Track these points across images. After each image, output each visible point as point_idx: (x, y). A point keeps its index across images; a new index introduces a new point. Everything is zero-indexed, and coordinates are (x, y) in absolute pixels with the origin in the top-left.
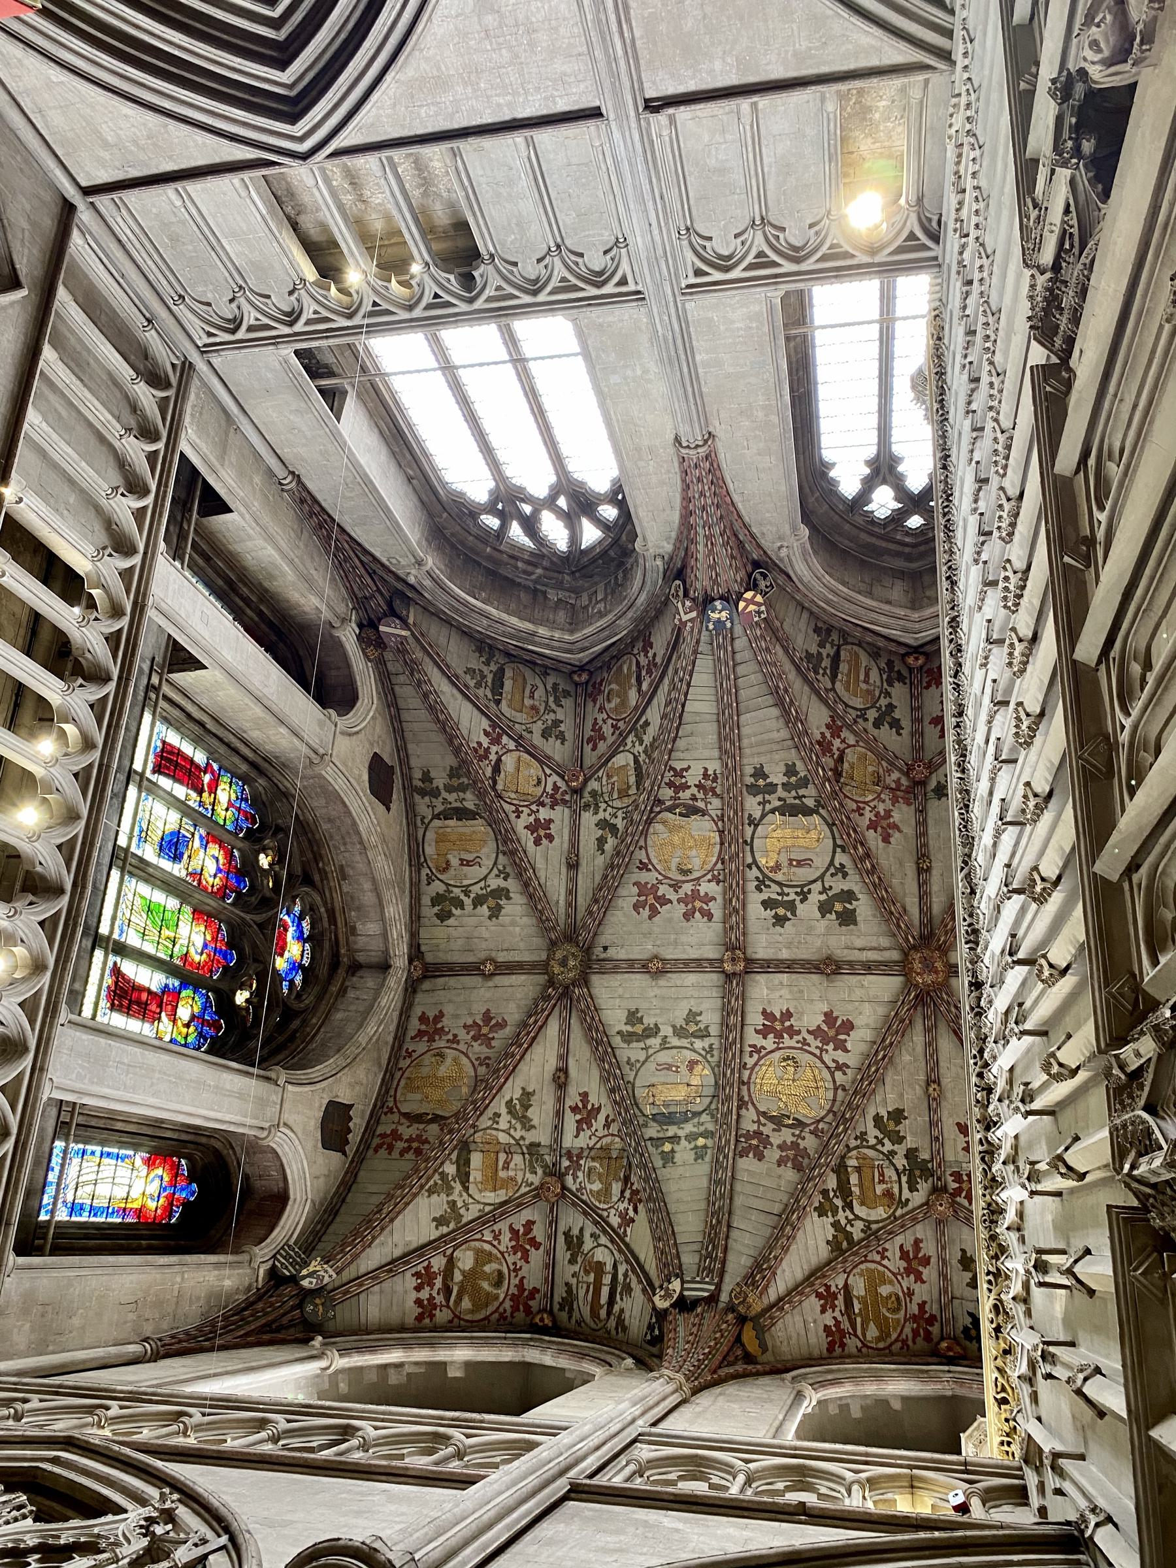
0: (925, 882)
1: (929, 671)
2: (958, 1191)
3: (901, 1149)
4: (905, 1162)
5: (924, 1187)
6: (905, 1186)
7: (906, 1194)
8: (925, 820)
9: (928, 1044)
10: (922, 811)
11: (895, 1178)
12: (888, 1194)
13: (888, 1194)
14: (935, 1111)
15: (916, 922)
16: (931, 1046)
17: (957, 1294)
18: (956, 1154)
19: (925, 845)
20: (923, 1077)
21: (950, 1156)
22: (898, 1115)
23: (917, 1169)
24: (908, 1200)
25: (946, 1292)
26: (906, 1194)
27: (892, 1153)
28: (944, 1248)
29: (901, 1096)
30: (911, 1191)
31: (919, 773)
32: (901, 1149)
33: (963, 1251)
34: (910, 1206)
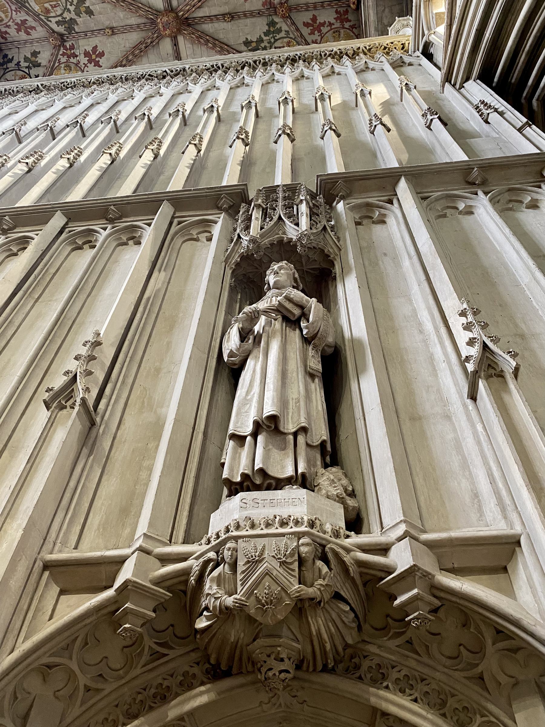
0: (218, 19)
1: (347, 12)
2: (65, 48)
3: (73, 15)
4: (68, 18)
5: (61, 29)
6: (57, 19)
7: (54, 20)
8: (254, 16)
9: (131, 26)
10: (259, 14)
11: (58, 13)
12: (48, 11)
13: (48, 11)
14: (99, 33)
15: (195, 15)
16: (128, 29)
17: (21, 50)
18: (83, 46)
19: (239, 18)
20: (115, 25)
21: (81, 42)
22: (89, 12)
23: (70, 24)
24: (51, 21)
25: (20, 44)
26: (54, 20)
27: (69, 11)
28: (37, 42)
29: (100, 13)
30: (56, 22)
31: (280, 11)
32: (73, 15)
33: (39, 53)
34: (49, 23)
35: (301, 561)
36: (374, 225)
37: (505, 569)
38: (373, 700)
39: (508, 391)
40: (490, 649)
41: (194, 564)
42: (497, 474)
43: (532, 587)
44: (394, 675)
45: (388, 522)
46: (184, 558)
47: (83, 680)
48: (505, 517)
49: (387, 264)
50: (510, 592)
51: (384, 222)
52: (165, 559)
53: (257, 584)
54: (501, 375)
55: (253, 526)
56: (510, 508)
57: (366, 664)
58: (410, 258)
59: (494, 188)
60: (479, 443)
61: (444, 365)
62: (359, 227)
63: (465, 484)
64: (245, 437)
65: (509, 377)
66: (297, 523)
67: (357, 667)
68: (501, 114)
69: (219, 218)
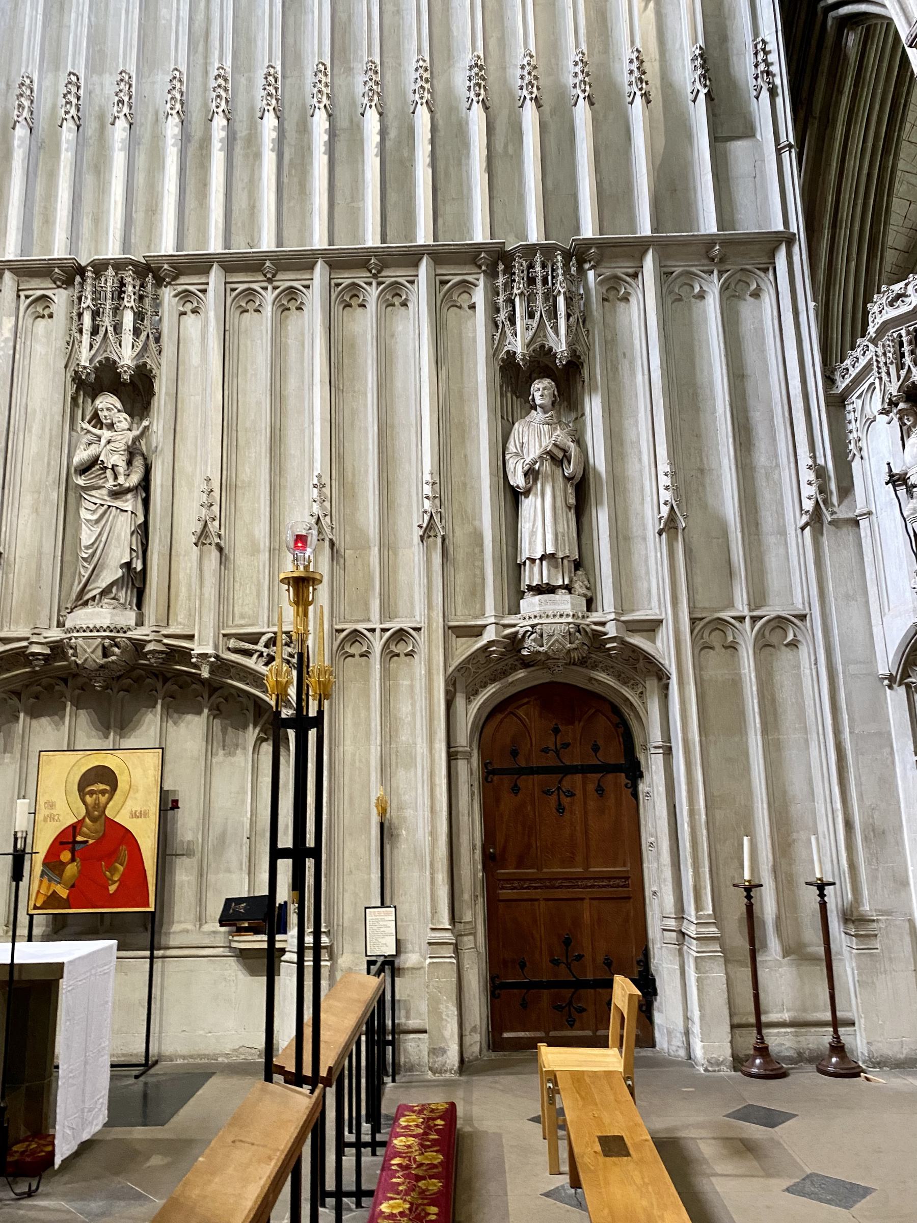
35: (570, 634)
36: (618, 302)
37: (654, 630)
38: (592, 675)
39: (677, 539)
40: (641, 661)
41: (522, 631)
42: (661, 585)
43: (663, 641)
44: (601, 665)
45: (607, 609)
46: (514, 626)
47: (473, 670)
48: (660, 608)
49: (625, 365)
50: (654, 641)
51: (628, 300)
52: (506, 626)
53: (552, 645)
54: (676, 528)
55: (548, 616)
56: (662, 605)
57: (589, 661)
58: (643, 374)
59: (728, 267)
60: (657, 563)
61: (649, 499)
62: (606, 303)
63: (645, 585)
64: (535, 560)
65: (680, 531)
66: (568, 615)
67: (586, 662)
68: (773, 92)
69: (478, 280)
